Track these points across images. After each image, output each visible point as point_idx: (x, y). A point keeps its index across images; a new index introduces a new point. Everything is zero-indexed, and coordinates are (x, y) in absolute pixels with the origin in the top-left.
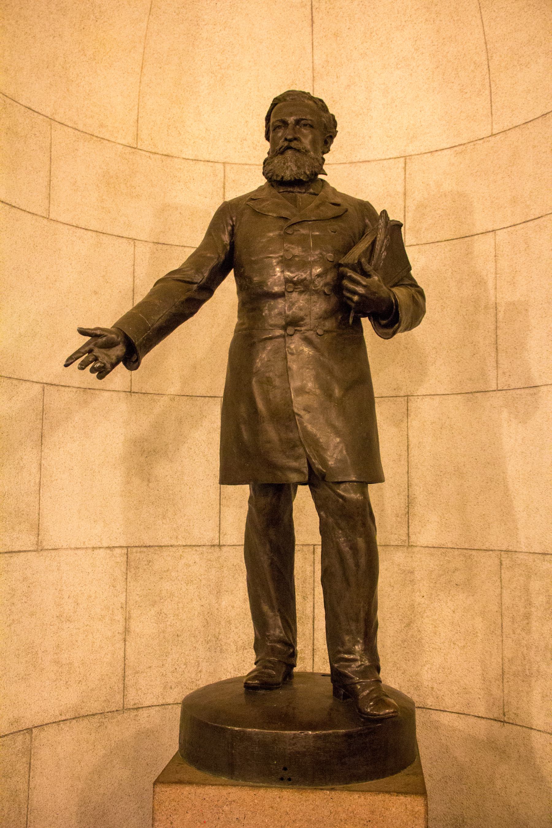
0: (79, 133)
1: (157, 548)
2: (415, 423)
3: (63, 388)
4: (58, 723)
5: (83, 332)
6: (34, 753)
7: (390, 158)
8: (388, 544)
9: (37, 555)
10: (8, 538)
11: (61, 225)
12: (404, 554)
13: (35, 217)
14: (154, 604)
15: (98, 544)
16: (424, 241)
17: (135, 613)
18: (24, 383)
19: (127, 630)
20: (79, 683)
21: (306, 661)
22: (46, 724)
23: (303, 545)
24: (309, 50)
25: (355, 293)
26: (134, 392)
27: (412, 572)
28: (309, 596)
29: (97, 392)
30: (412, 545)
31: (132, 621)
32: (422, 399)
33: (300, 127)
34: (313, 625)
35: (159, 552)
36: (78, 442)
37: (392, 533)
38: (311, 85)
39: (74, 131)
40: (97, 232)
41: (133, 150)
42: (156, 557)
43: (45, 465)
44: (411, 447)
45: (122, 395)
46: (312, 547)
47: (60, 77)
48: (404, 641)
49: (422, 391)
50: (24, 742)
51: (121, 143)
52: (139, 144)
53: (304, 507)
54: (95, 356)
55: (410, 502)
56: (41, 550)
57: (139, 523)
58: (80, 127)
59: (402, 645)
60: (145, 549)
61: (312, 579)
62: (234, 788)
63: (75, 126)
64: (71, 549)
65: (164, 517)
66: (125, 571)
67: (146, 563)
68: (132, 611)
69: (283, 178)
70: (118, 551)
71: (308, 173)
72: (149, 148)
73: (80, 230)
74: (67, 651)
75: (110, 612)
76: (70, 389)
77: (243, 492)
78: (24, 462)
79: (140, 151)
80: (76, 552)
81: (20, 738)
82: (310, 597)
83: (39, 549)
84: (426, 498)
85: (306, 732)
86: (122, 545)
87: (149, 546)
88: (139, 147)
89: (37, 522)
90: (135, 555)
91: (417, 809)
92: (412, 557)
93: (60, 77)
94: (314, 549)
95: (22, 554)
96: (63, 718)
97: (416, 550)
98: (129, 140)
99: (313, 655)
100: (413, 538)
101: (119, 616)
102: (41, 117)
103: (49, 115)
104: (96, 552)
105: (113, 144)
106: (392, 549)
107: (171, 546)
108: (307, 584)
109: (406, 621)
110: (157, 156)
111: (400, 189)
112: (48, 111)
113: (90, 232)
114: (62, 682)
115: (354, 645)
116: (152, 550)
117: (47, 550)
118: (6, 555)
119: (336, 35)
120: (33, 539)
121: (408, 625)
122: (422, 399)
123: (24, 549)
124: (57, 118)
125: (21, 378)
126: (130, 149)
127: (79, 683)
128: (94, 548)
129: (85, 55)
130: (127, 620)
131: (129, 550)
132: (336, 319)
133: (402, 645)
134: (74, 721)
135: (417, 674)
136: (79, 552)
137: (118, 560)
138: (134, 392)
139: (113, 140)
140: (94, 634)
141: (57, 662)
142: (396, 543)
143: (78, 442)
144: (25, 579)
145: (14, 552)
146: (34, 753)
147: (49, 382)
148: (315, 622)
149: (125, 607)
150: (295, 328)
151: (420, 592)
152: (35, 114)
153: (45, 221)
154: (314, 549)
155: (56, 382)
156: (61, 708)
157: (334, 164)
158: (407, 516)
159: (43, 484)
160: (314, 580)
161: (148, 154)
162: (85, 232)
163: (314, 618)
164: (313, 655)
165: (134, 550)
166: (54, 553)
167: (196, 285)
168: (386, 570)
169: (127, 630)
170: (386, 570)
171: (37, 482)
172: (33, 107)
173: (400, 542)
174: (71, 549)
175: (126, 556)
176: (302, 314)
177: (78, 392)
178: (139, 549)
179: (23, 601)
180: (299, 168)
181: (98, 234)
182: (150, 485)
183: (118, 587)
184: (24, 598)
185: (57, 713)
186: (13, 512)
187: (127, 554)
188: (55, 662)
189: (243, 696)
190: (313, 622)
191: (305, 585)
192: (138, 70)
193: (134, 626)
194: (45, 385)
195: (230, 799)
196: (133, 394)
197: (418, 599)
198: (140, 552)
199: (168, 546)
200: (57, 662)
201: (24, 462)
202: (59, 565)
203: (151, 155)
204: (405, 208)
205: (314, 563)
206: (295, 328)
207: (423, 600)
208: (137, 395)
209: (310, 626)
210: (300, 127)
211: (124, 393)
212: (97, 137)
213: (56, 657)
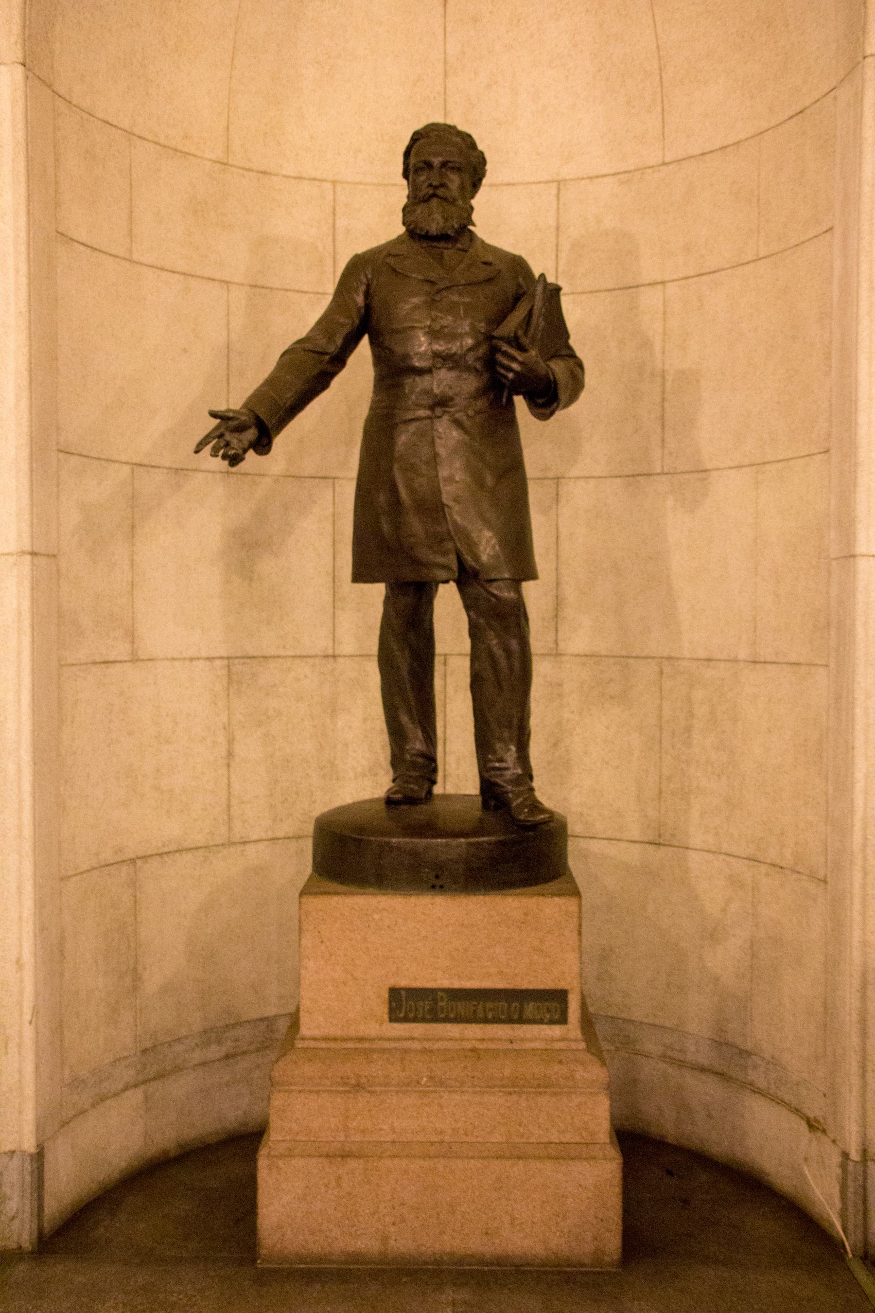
4: (160, 855)
5: (214, 415)
14: (260, 724)
16: (580, 290)
19: (230, 754)
24: (441, 37)
27: (561, 685)
29: (190, 473)
33: (443, 166)
41: (223, 167)
45: (218, 476)
49: (574, 472)
58: (162, 141)
64: (167, 659)
66: (226, 685)
69: (428, 231)
70: (218, 663)
71: (456, 226)
76: (161, 470)
77: (377, 591)
81: (124, 868)
83: (135, 659)
91: (571, 909)
95: (118, 664)
96: (166, 850)
100: (562, 645)
101: (221, 739)
102: (119, 132)
104: (195, 663)
107: (278, 657)
111: (552, 222)
112: (126, 124)
121: (555, 745)
124: (137, 131)
126: (219, 165)
128: (192, 659)
130: (231, 741)
134: (178, 854)
135: (565, 799)
136: (176, 663)
141: (157, 788)
149: (227, 727)
152: (113, 129)
153: (127, 264)
155: (145, 462)
161: (241, 171)
162: (172, 275)
165: (236, 661)
166: (150, 664)
169: (230, 754)
172: (110, 120)
174: (167, 659)
176: (450, 393)
178: (242, 661)
180: (446, 220)
185: (160, 844)
187: (229, 666)
193: (240, 750)
200: (157, 788)
203: (246, 173)
210: (443, 166)
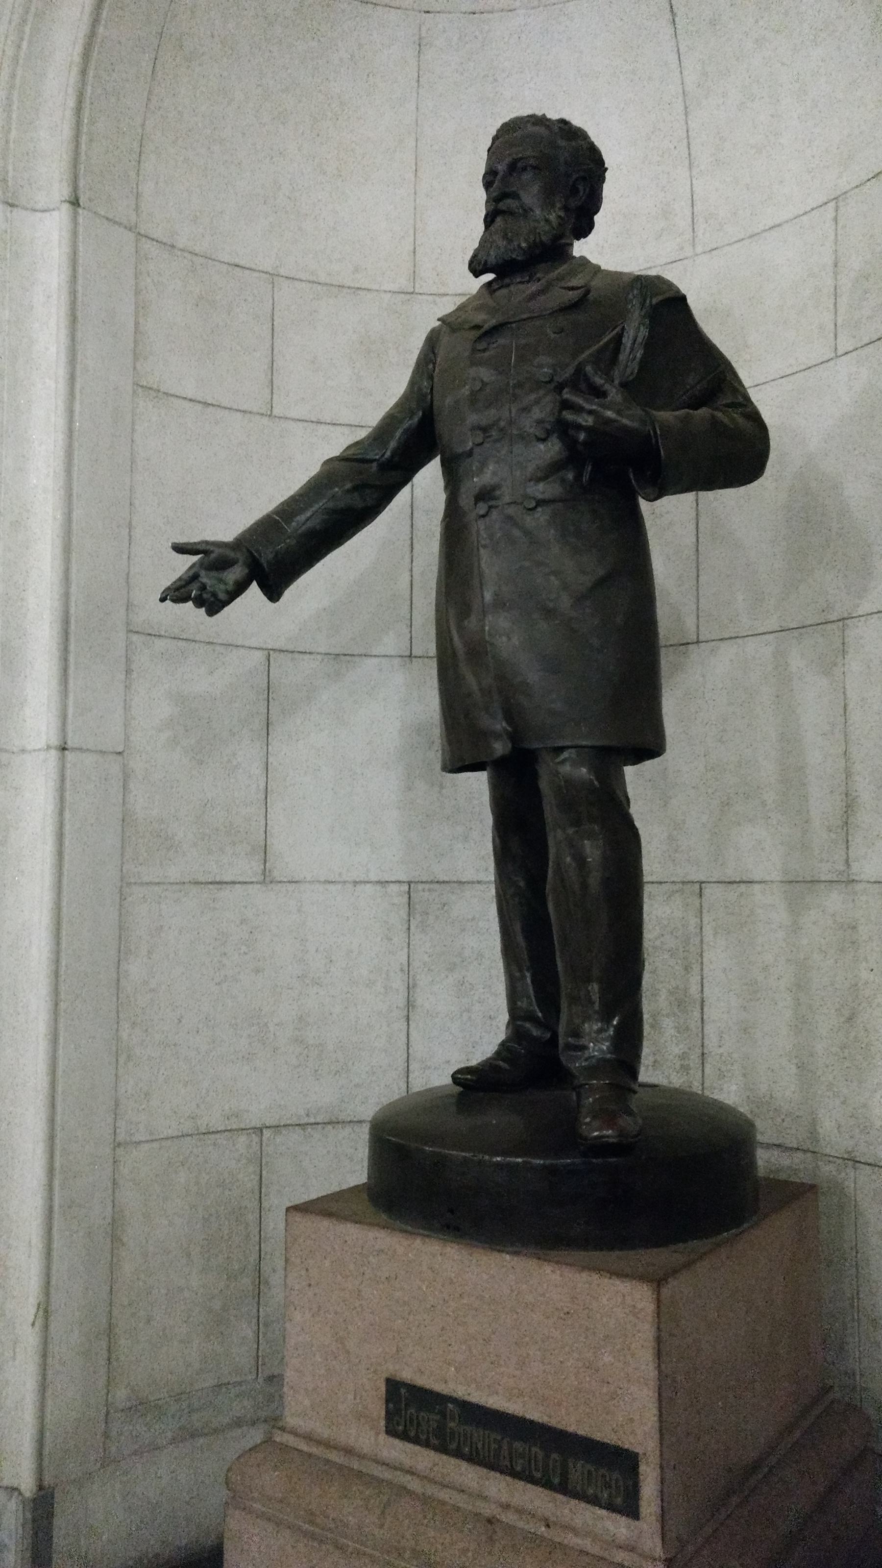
0: (319, 287)
1: (456, 885)
2: (854, 665)
3: (301, 656)
4: (303, 1126)
5: (181, 549)
6: (267, 1162)
7: (813, 209)
8: (816, 878)
9: (264, 889)
10: (213, 863)
11: (291, 422)
12: (843, 895)
13: (248, 416)
14: (452, 968)
15: (363, 877)
16: (866, 340)
17: (423, 980)
18: (234, 651)
19: (410, 1004)
20: (336, 1074)
21: (691, 1072)
22: (284, 1126)
23: (683, 883)
24: (674, 64)
25: (579, 427)
26: (415, 657)
27: (854, 928)
28: (694, 966)
29: (357, 659)
30: (853, 880)
31: (418, 990)
32: (865, 622)
34: (702, 1013)
35: (459, 891)
36: (327, 732)
37: (821, 861)
38: (683, 123)
39: (311, 285)
40: (351, 425)
41: (408, 297)
42: (454, 898)
43: (275, 763)
44: (849, 708)
45: (397, 661)
46: (697, 886)
47: (287, 212)
48: (843, 1047)
49: (866, 607)
50: (249, 1146)
51: (388, 289)
52: (417, 285)
53: (684, 822)
54: (202, 583)
55: (850, 805)
56: (271, 882)
57: (427, 847)
58: (323, 278)
59: (841, 1054)
60: (436, 886)
61: (699, 939)
62: (382, 1231)
63: (311, 278)
64: (319, 882)
65: (466, 839)
66: (406, 917)
67: (439, 906)
68: (418, 977)
69: (486, 261)
70: (394, 888)
71: (524, 245)
72: (434, 290)
73: (323, 426)
74: (315, 1027)
75: (384, 976)
76: (312, 657)
78: (239, 760)
79: (419, 296)
80: (327, 886)
81: (243, 1139)
82: (696, 968)
83: (267, 879)
84: (874, 795)
85: (480, 1156)
86: (401, 879)
87: (444, 882)
88: (417, 291)
89: (263, 843)
90: (421, 894)
91: (640, 1306)
92: (854, 900)
93: (287, 212)
94: (701, 889)
95: (237, 886)
96: (312, 1120)
97: (859, 887)
98: (403, 283)
99: (703, 1063)
100: (855, 867)
101: (398, 983)
102: (256, 274)
103: (270, 270)
104: (360, 888)
105: (375, 294)
106: (823, 887)
107: (479, 882)
108: (691, 945)
109: (846, 1013)
110: (448, 298)
111: (829, 260)
112: (267, 265)
113: (339, 427)
114: (308, 1069)
115: (583, 1023)
116: (447, 887)
117: (280, 882)
118: (211, 886)
119: (713, 23)
120: (259, 868)
121: (850, 1019)
122: (865, 622)
123: (241, 880)
124: (282, 272)
125: (230, 642)
126: (403, 295)
127: (336, 1074)
128: (355, 883)
129: (324, 174)
130: (410, 988)
131: (412, 885)
132: (563, 481)
133: (841, 1054)
134: (330, 1127)
135: (865, 1106)
136: (332, 887)
137: (396, 901)
138: (415, 657)
139: (375, 287)
140: (359, 1007)
141: (298, 1041)
142: (829, 877)
143: (327, 732)
144: (243, 921)
145: (226, 883)
146: (267, 1162)
147: (276, 647)
148: (705, 1009)
149: (408, 969)
150: (490, 503)
151: (867, 962)
152: (247, 272)
153: (265, 421)
154: (701, 889)
155: (290, 647)
156: (309, 1106)
157: (723, 246)
158: (845, 829)
159: (272, 791)
160: (702, 941)
161: (430, 298)
162: (331, 428)
163: (703, 1001)
164: (703, 1063)
165: (420, 887)
166: (291, 887)
167: (375, 464)
168: (814, 923)
169: (410, 1004)
170: (814, 923)
171: (261, 787)
172: (242, 263)
173: (834, 875)
174: (319, 882)
175: (407, 896)
176: (496, 480)
177: (326, 660)
178: (427, 886)
179: (242, 951)
180: (510, 241)
181: (353, 429)
182: (444, 791)
183: (395, 940)
184: (244, 948)
185: (302, 1112)
186: (222, 827)
187: (409, 893)
188: (296, 1040)
189: (454, 1100)
190: (702, 1009)
191: (687, 948)
192: (410, 176)
193: (421, 999)
194: (271, 652)
195: (377, 1247)
196: (414, 660)
197: (864, 975)
198: (429, 890)
199: (473, 882)
200: (298, 1041)
201: (239, 760)
202: (299, 904)
203: (437, 299)
204: (836, 289)
205: (701, 912)
206: (490, 503)
207: (872, 977)
208: (420, 660)
209: (697, 1014)
211: (399, 659)
212: (349, 288)
213: (297, 1032)
